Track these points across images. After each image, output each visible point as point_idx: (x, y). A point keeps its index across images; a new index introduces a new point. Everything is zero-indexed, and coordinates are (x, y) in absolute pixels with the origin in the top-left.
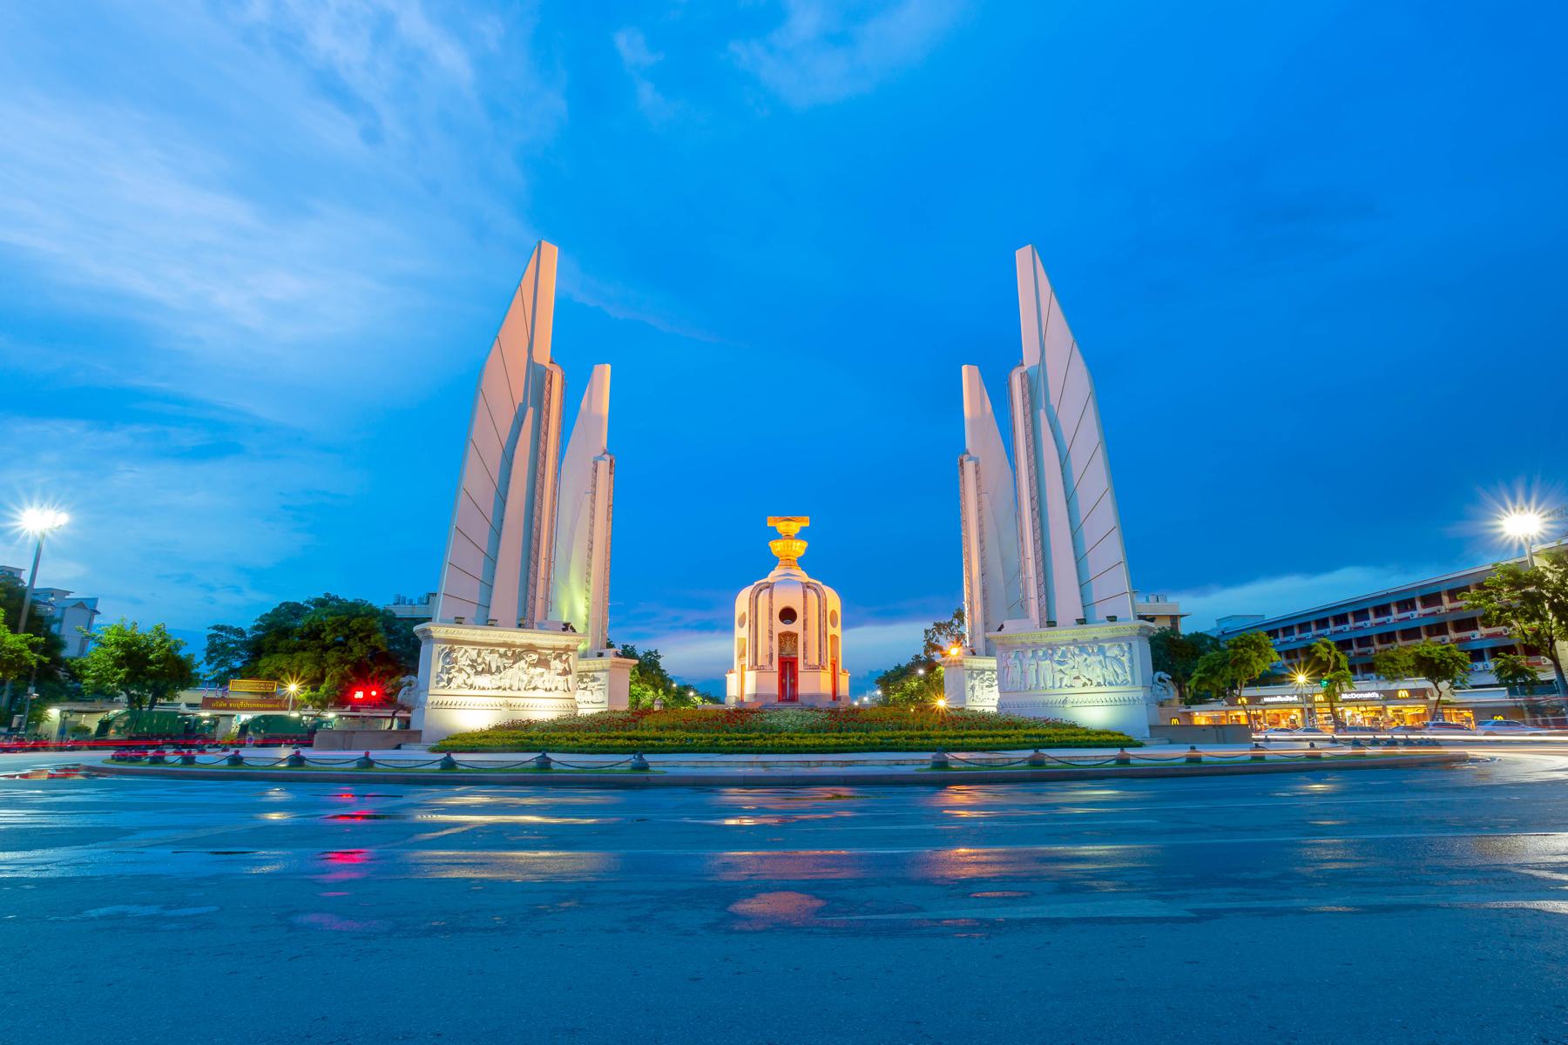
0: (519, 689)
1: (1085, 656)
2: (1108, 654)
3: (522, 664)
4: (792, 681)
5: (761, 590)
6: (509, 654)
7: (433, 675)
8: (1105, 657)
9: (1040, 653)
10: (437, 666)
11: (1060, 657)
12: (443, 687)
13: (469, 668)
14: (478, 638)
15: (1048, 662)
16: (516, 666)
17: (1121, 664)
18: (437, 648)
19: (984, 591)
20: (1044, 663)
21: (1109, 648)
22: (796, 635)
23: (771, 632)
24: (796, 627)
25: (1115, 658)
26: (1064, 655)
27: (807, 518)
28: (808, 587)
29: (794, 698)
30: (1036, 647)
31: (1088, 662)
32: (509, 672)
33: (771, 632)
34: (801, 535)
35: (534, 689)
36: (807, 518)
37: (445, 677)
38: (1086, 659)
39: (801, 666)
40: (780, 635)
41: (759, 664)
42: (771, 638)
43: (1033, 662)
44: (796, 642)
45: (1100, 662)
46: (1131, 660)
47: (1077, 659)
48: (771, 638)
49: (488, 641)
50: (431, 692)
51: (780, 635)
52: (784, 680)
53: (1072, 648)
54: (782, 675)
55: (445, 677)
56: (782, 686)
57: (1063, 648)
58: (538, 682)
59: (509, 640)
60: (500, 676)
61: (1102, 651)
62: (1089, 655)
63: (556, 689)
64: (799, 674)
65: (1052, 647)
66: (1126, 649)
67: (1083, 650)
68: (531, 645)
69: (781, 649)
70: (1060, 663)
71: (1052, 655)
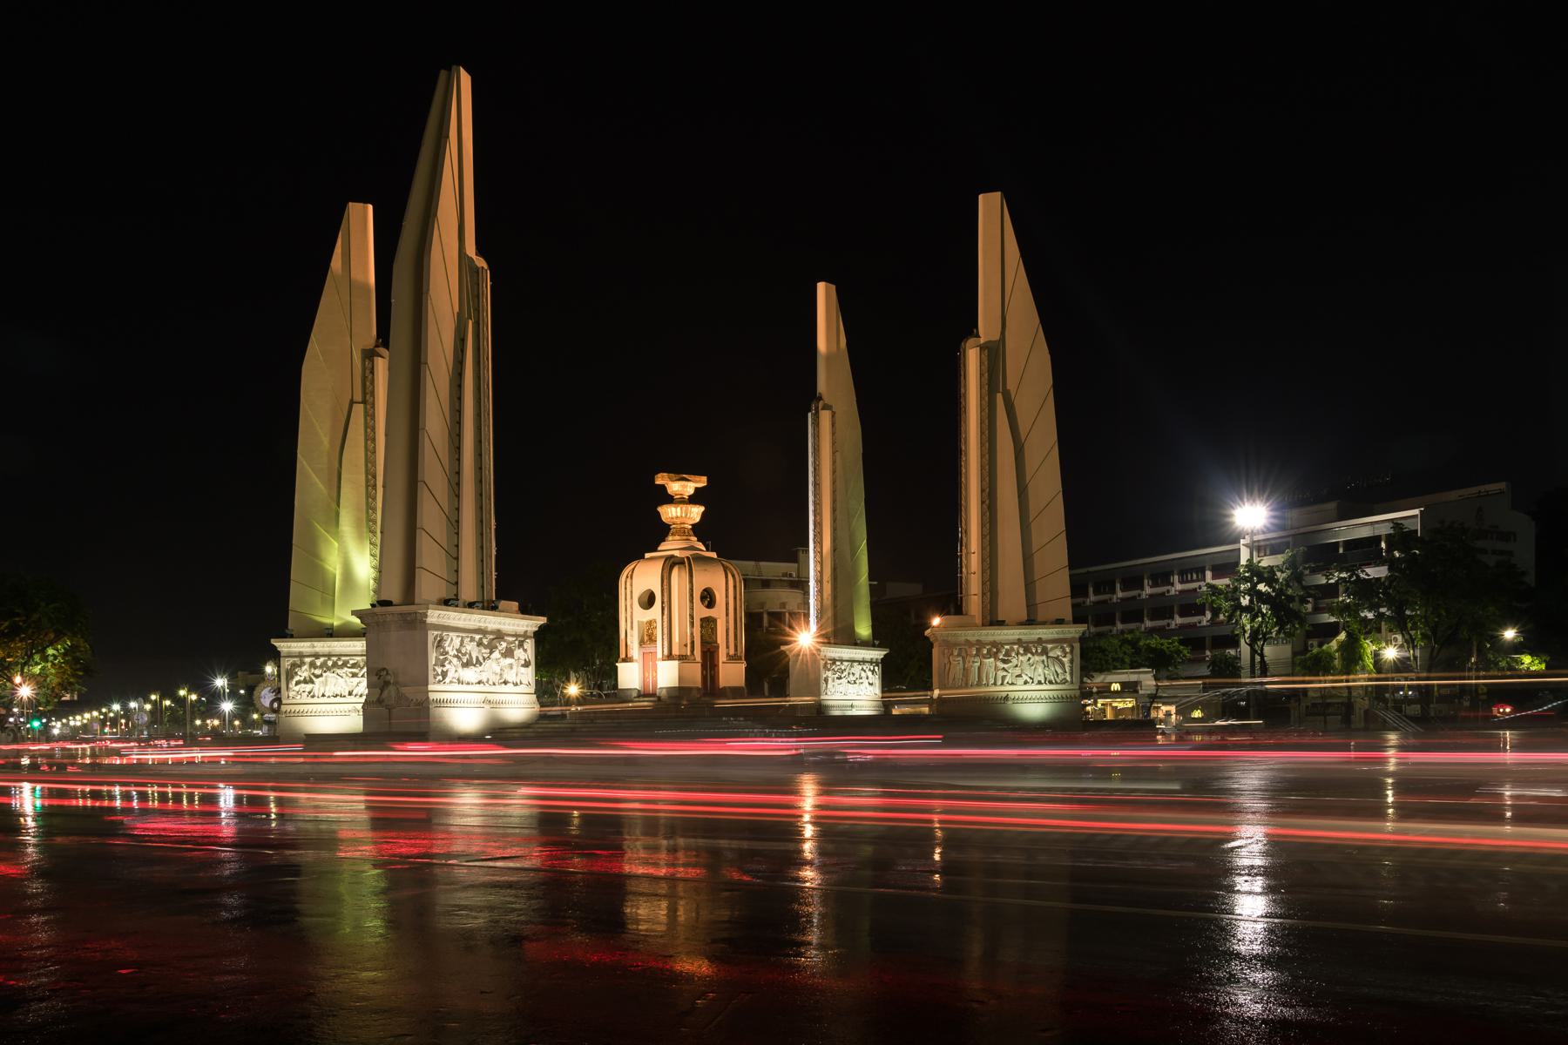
0: (494, 684)
1: (1029, 655)
2: (1051, 654)
3: (496, 654)
6: (485, 642)
7: (430, 668)
8: (1048, 657)
9: (985, 652)
10: (433, 656)
11: (1004, 656)
12: (439, 681)
13: (456, 659)
14: (461, 624)
15: (992, 660)
16: (493, 656)
17: (1062, 665)
18: (432, 634)
19: (834, 569)
20: (988, 660)
21: (1052, 649)
23: (692, 617)
25: (1057, 658)
26: (1008, 654)
30: (980, 644)
31: (1031, 661)
32: (488, 662)
35: (505, 683)
36: (704, 479)
37: (439, 670)
38: (1029, 659)
40: (701, 620)
41: (676, 651)
43: (977, 659)
45: (1043, 661)
46: (1072, 661)
47: (1021, 658)
48: (692, 624)
49: (467, 627)
50: (431, 687)
51: (701, 620)
53: (1015, 647)
54: (704, 667)
55: (439, 670)
56: (704, 678)
57: (1006, 647)
58: (510, 676)
59: (483, 625)
60: (481, 668)
61: (1045, 652)
62: (1033, 654)
63: (521, 683)
65: (997, 645)
66: (1068, 650)
67: (1027, 650)
68: (499, 631)
70: (1004, 661)
71: (996, 653)
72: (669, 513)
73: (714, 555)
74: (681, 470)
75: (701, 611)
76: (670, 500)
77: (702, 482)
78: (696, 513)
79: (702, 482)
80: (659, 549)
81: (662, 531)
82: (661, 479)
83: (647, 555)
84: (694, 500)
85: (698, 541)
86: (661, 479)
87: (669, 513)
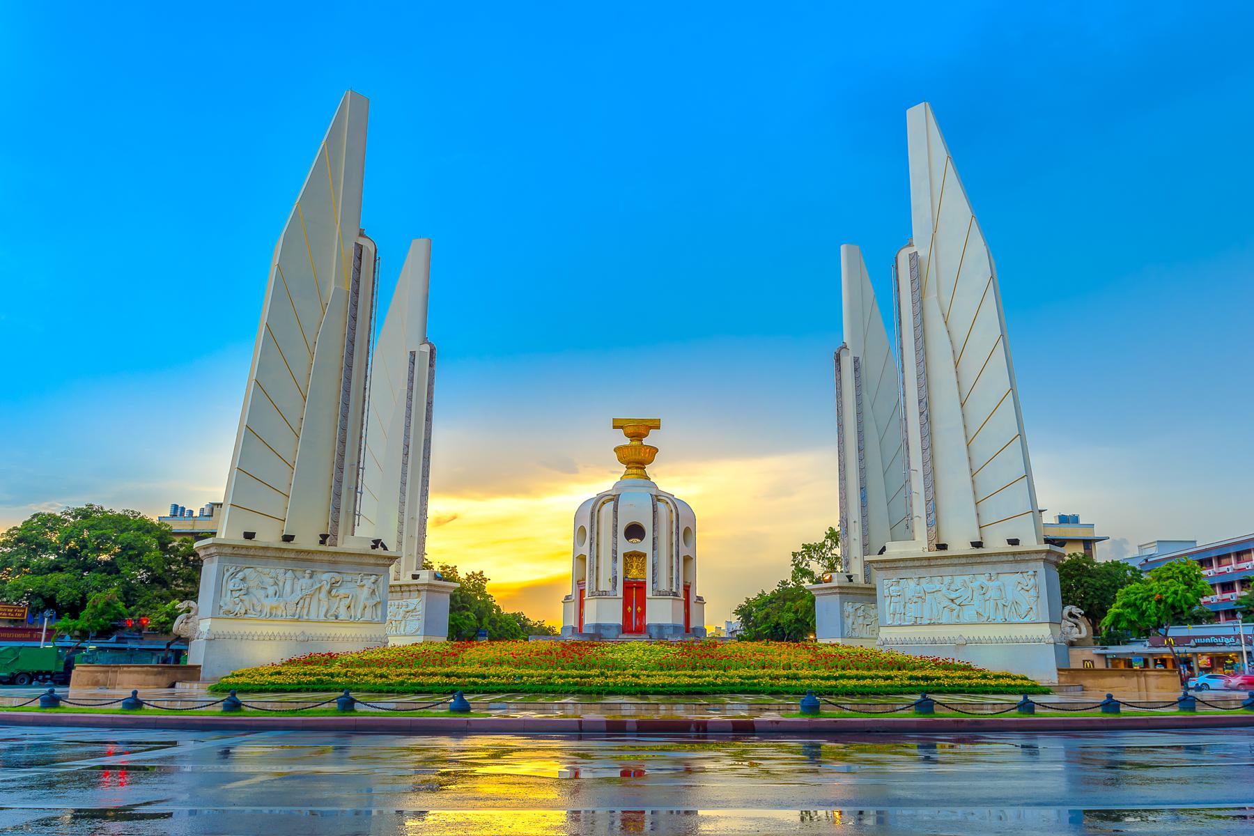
4: (639, 609)
5: (604, 503)
22: (645, 555)
24: (644, 546)
28: (659, 500)
29: (641, 630)
33: (615, 552)
39: (649, 594)
40: (625, 555)
42: (615, 559)
44: (644, 564)
48: (615, 559)
51: (625, 555)
52: (629, 609)
54: (627, 601)
64: (647, 600)
69: (626, 571)
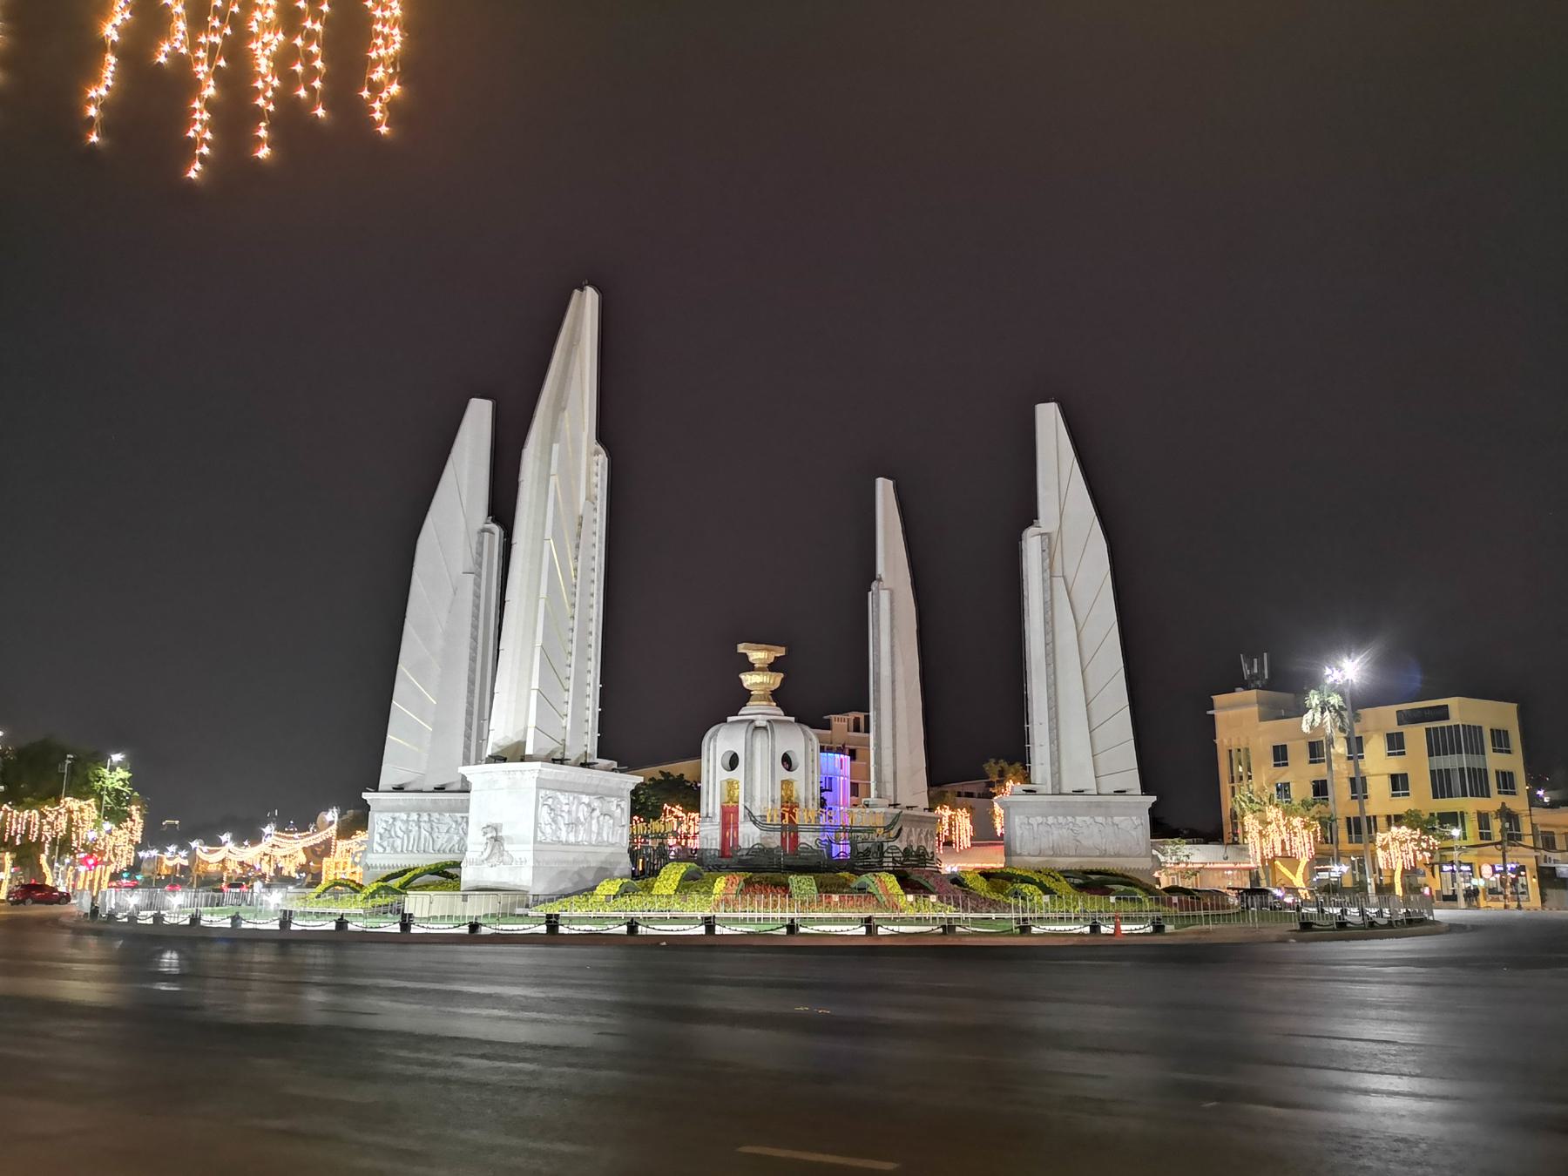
27: (784, 649)
34: (773, 667)
36: (784, 649)
72: (749, 680)
73: (792, 719)
74: (758, 640)
75: (782, 773)
76: (751, 668)
77: (780, 652)
78: (774, 680)
79: (780, 652)
80: (741, 712)
81: (745, 696)
82: (741, 648)
83: (730, 719)
84: (773, 667)
85: (777, 706)
86: (741, 648)
87: (749, 680)
